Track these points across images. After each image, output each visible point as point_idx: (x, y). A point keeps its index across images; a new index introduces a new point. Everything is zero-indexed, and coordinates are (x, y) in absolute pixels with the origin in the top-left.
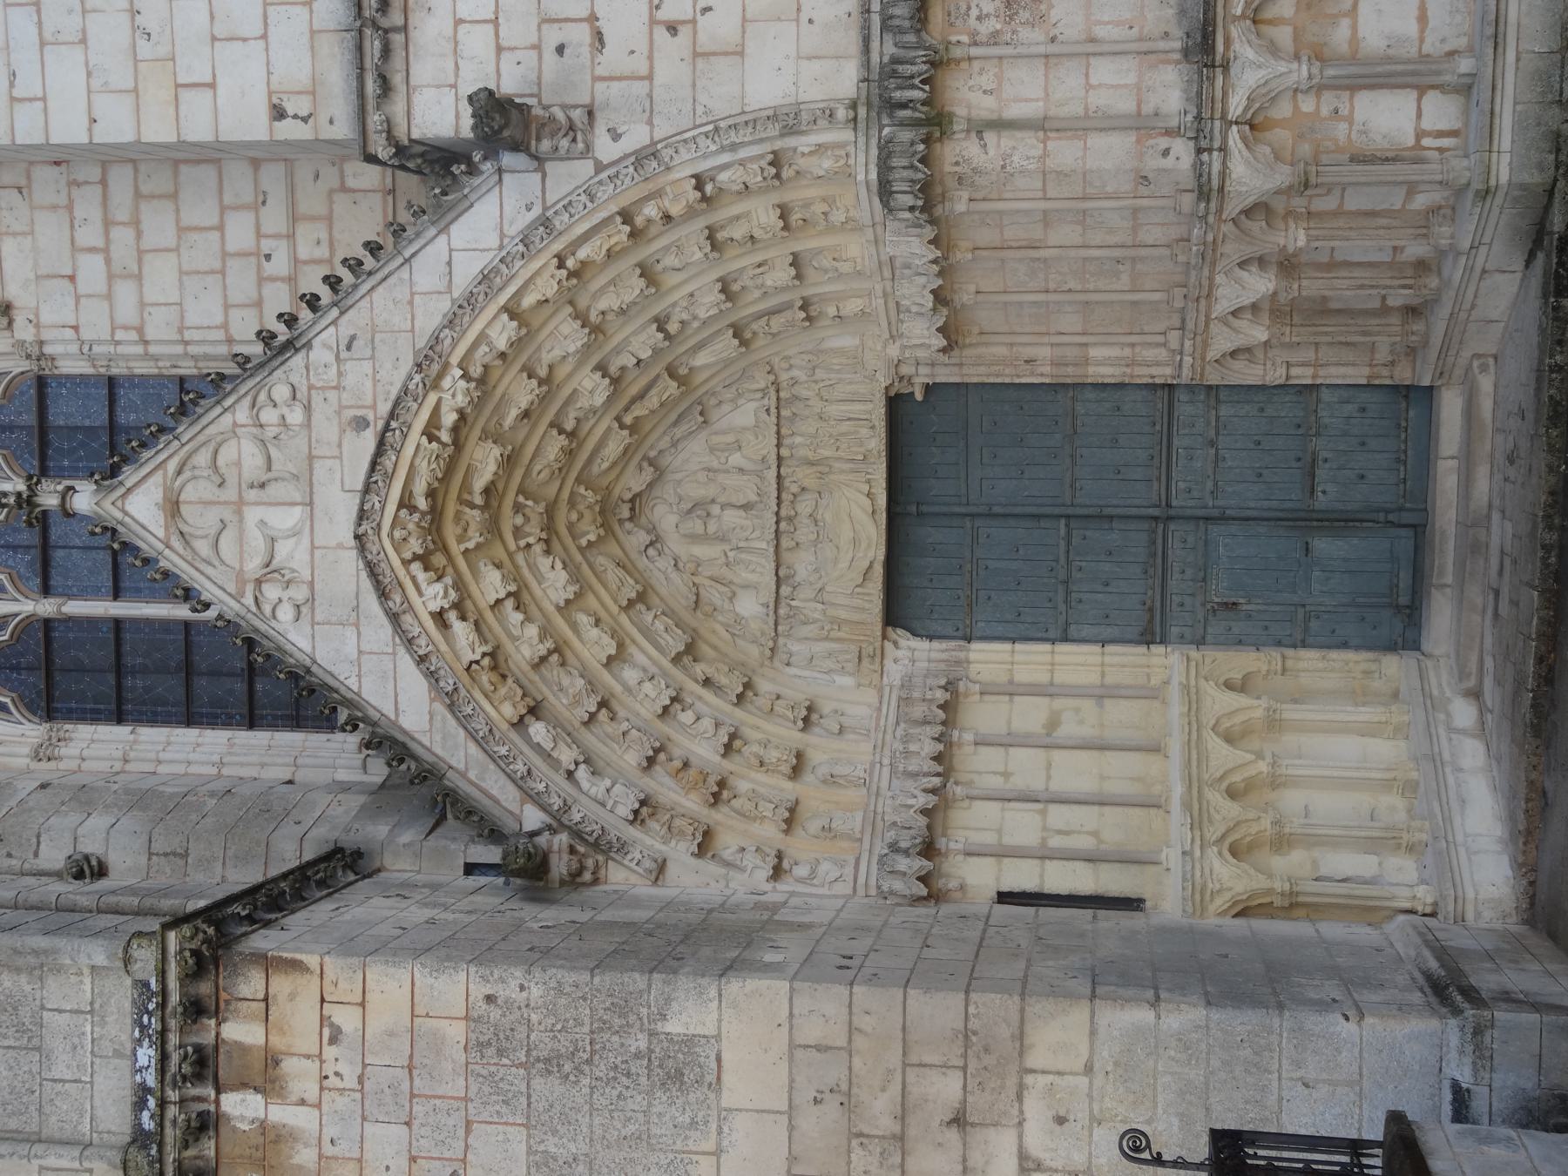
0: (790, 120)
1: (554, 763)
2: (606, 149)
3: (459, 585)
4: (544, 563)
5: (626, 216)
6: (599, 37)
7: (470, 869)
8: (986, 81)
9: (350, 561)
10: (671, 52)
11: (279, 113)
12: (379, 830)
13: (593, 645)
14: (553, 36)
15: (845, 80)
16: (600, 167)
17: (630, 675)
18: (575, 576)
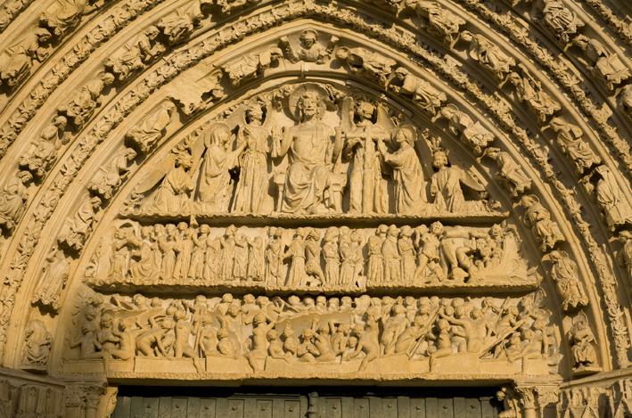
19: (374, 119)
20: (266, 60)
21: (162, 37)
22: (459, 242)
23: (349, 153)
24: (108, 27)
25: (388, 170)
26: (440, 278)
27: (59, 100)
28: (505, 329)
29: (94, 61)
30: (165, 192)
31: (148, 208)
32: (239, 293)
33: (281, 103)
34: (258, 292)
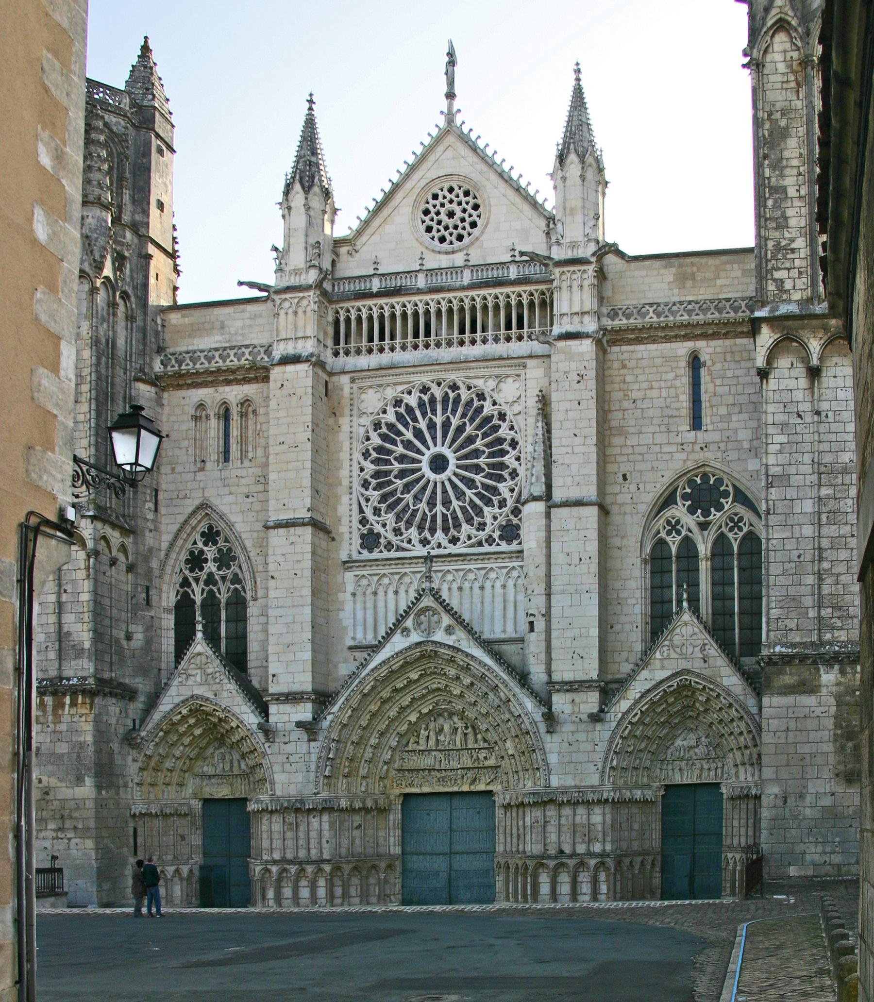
0: (273, 783)
1: (156, 737)
2: (267, 745)
3: (188, 716)
4: (201, 729)
5: (255, 749)
6: (285, 743)
7: (134, 720)
8: (278, 820)
9: (190, 694)
10: (282, 758)
11: (274, 676)
12: (142, 698)
13: (187, 740)
14: (287, 734)
15: (279, 793)
16: (263, 744)
17: (181, 748)
18: (200, 736)
19: (462, 719)
20: (431, 708)
21: (402, 707)
22: (482, 754)
23: (457, 729)
24: (388, 707)
25: (466, 734)
26: (476, 765)
27: (379, 728)
28: (492, 777)
29: (387, 716)
30: (410, 744)
31: (406, 749)
32: (429, 770)
33: (440, 715)
34: (434, 770)
